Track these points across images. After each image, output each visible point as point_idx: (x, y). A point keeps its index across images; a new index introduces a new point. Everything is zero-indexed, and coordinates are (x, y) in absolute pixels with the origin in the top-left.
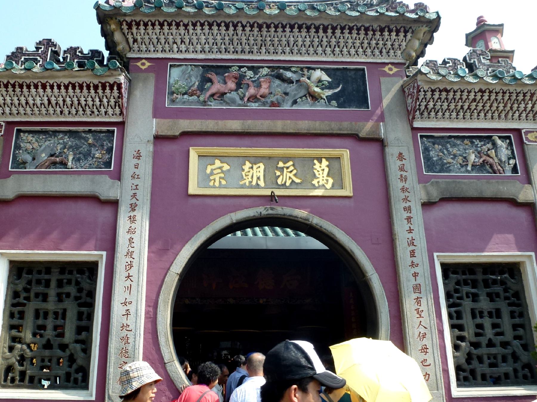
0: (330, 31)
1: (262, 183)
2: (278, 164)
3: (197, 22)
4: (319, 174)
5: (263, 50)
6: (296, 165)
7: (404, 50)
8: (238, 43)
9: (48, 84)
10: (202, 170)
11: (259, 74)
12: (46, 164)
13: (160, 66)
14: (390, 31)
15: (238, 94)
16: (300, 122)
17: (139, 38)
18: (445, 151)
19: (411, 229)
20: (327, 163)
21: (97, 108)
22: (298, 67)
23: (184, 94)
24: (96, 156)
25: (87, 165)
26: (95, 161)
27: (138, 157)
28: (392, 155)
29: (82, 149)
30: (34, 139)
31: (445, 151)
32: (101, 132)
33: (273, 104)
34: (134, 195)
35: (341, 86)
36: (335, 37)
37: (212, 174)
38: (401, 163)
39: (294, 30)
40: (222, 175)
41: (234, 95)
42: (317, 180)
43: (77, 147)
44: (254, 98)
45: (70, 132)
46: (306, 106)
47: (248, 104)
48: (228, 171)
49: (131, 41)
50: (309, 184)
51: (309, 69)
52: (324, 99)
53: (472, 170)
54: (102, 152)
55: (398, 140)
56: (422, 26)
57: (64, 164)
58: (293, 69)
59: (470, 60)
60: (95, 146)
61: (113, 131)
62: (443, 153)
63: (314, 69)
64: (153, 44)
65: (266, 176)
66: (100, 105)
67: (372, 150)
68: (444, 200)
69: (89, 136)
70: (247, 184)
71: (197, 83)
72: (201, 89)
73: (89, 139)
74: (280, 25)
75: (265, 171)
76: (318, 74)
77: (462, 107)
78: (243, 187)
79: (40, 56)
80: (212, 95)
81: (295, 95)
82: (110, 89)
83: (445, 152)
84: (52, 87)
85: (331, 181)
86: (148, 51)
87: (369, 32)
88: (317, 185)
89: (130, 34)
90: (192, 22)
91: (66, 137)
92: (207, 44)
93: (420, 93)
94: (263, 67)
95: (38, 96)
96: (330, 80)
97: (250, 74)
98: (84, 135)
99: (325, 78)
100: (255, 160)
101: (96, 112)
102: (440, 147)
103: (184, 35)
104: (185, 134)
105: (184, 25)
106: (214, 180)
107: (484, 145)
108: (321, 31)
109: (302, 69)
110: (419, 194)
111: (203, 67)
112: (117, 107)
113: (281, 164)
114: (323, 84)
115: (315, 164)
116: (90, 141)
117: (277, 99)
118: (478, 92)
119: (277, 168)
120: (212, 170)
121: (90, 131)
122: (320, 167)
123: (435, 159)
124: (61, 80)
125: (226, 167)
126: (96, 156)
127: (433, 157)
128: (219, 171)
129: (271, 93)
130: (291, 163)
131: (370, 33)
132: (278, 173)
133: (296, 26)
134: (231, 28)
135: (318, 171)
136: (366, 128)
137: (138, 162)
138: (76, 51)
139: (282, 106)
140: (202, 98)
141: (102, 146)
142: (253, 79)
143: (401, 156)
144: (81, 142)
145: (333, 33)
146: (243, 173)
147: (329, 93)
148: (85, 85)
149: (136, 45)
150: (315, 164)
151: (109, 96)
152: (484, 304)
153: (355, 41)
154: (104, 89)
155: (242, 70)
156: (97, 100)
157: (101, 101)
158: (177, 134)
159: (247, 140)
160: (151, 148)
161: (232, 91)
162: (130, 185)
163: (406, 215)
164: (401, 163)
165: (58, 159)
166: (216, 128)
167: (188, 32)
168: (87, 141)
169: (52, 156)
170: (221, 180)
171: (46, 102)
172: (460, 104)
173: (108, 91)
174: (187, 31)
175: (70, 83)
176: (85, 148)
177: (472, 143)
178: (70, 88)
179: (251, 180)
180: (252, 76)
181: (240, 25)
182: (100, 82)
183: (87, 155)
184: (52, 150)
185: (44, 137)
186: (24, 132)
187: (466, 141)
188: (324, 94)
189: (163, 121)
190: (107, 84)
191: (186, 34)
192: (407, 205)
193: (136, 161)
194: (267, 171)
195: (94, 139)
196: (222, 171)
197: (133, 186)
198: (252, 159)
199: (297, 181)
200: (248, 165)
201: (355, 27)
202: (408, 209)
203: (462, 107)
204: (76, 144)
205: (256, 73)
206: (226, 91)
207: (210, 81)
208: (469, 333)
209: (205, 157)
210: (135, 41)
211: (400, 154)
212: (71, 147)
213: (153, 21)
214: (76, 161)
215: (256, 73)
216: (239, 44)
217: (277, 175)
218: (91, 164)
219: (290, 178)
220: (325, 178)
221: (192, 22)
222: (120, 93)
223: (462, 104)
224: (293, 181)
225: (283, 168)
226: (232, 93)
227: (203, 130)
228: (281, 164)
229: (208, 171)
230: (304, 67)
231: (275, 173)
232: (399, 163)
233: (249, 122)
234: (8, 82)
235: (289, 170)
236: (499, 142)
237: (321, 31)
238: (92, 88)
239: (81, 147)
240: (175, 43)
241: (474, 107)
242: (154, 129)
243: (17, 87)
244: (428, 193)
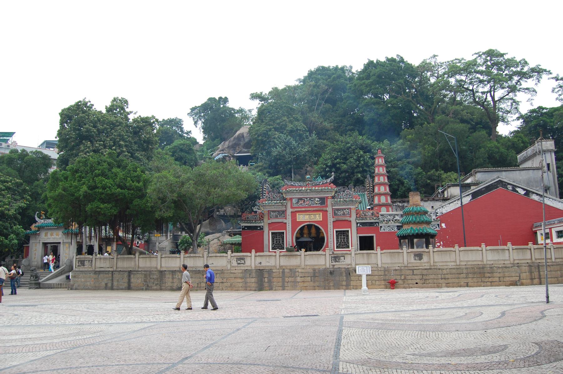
13: (291, 199)
19: (330, 226)
76: (317, 199)
110: (332, 220)
136: (324, 209)
152: (342, 237)
208: (339, 241)
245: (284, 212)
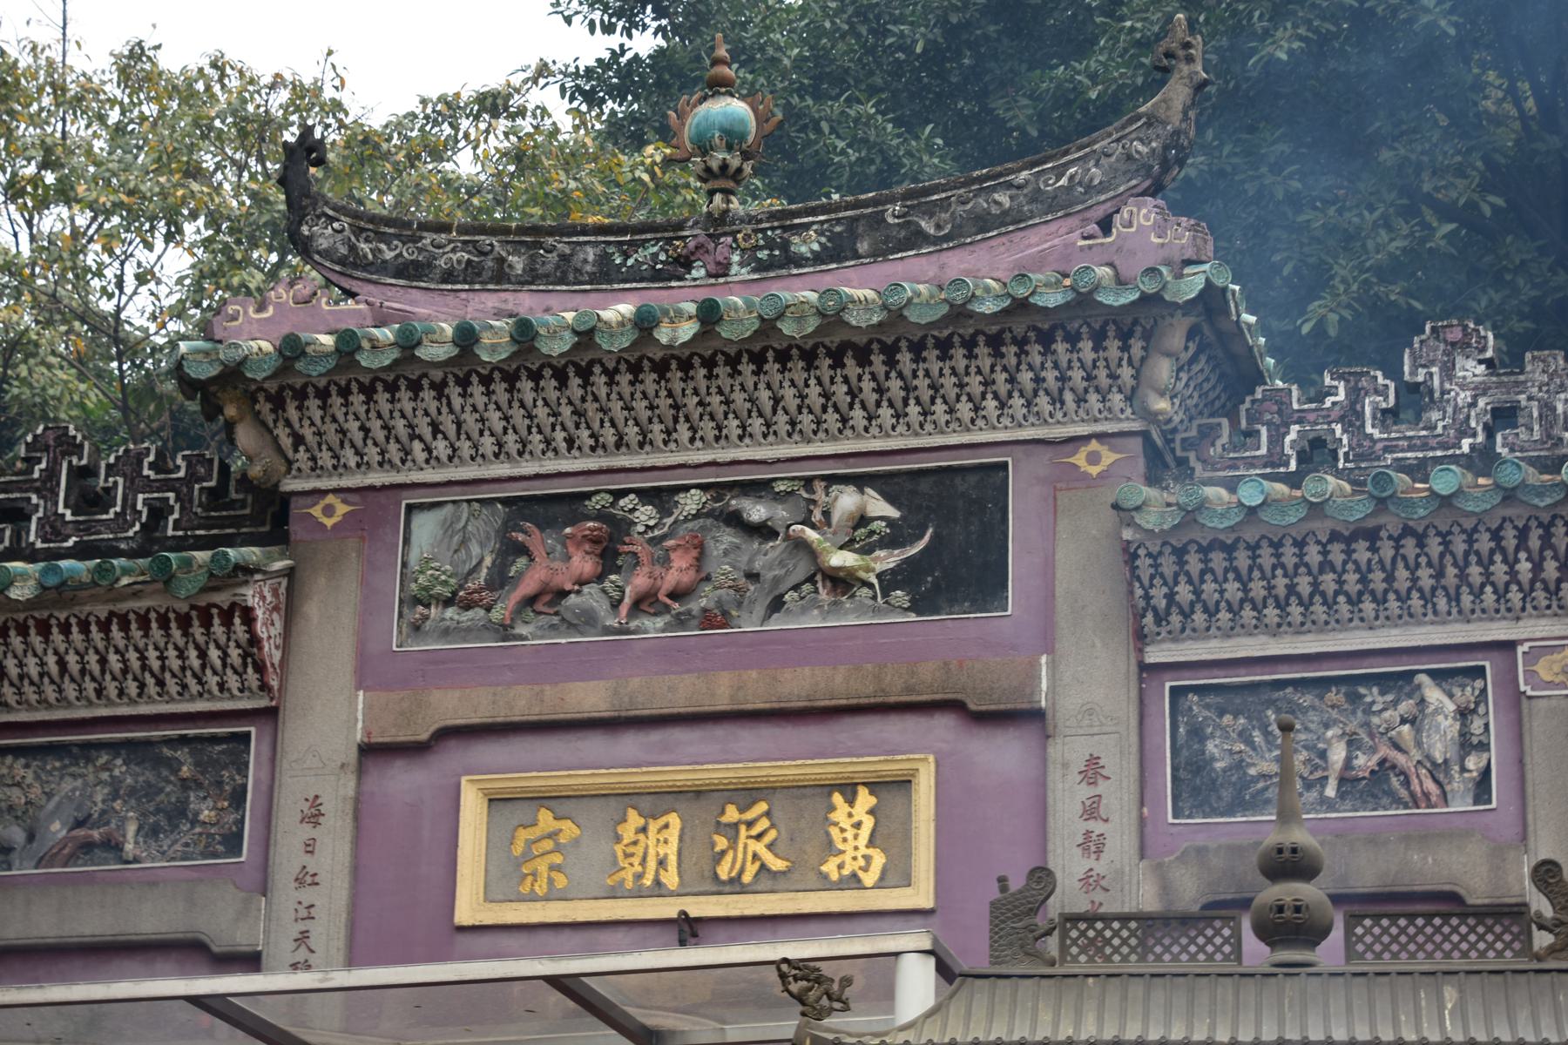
1: (671, 879)
2: (723, 812)
3: (469, 374)
4: (845, 840)
5: (683, 432)
6: (776, 814)
7: (1134, 389)
8: (602, 421)
9: (53, 621)
10: (496, 844)
11: (676, 512)
12: (66, 851)
15: (604, 591)
16: (787, 674)
17: (308, 432)
18: (1256, 733)
20: (873, 801)
21: (195, 675)
22: (793, 479)
23: (448, 602)
24: (202, 817)
25: (178, 847)
26: (200, 834)
27: (314, 817)
28: (1065, 765)
29: (162, 797)
31: (1256, 733)
32: (214, 739)
33: (708, 620)
34: (303, 937)
35: (930, 531)
36: (900, 375)
37: (527, 857)
38: (1092, 791)
39: (766, 367)
40: (557, 859)
41: (592, 598)
42: (837, 860)
43: (150, 791)
44: (645, 603)
47: (633, 624)
48: (576, 842)
49: (286, 442)
50: (812, 876)
51: (832, 480)
52: (871, 586)
53: (1342, 795)
54: (219, 805)
55: (1090, 712)
56: (1172, 316)
57: (112, 846)
58: (781, 487)
59: (1413, 373)
60: (199, 786)
61: (248, 734)
62: (1249, 742)
64: (353, 446)
65: (685, 853)
66: (203, 666)
69: (182, 754)
70: (629, 884)
71: (488, 561)
72: (500, 580)
73: (181, 764)
74: (720, 358)
75: (681, 839)
77: (1291, 589)
78: (614, 894)
79: (37, 491)
80: (530, 601)
81: (777, 581)
82: (222, 624)
83: (1258, 737)
84: (65, 629)
85: (879, 860)
86: (339, 467)
87: (1004, 349)
88: (834, 876)
89: (281, 424)
90: (455, 376)
91: (119, 762)
92: (510, 431)
93: (1138, 563)
94: (686, 488)
95: (29, 654)
96: (893, 513)
97: (645, 514)
98: (167, 752)
99: (879, 507)
100: (656, 801)
101: (194, 687)
102: (1242, 721)
103: (440, 413)
104: (449, 733)
105: (433, 386)
106: (534, 874)
107: (1395, 703)
108: (849, 362)
109: (808, 482)
111: (506, 502)
112: (250, 670)
113: (732, 814)
114: (872, 533)
115: (832, 808)
116: (185, 771)
117: (719, 603)
118: (1330, 541)
119: (720, 828)
121: (184, 740)
122: (850, 815)
123: (1219, 765)
124: (87, 608)
125: (569, 829)
126: (202, 817)
127: (1213, 759)
128: (548, 845)
129: (708, 578)
130: (762, 807)
132: (721, 843)
133: (770, 355)
134: (575, 382)
135: (843, 830)
137: (314, 833)
138: (140, 463)
139: (735, 622)
140: (496, 615)
141: (219, 784)
142: (657, 533)
143: (1093, 770)
144: (159, 775)
145: (891, 363)
146: (619, 849)
147: (887, 560)
148: (153, 615)
149: (302, 454)
150: (832, 808)
151: (222, 639)
153: (966, 380)
154: (207, 624)
155: (622, 503)
156: (193, 654)
157: (203, 655)
159: (630, 743)
160: (349, 785)
161: (587, 582)
162: (292, 905)
164: (1092, 791)
165: (96, 834)
166: (537, 710)
167: (449, 404)
168: (176, 771)
169: (79, 824)
170: (553, 874)
171: (53, 668)
172: (1281, 582)
173: (218, 629)
174: (444, 401)
175: (112, 614)
177: (1355, 698)
178: (114, 628)
179: (640, 869)
180: (652, 523)
181: (597, 369)
182: (193, 607)
183: (179, 813)
184: (78, 809)
185: (57, 764)
187: (1333, 696)
188: (868, 570)
190: (215, 611)
191: (445, 410)
193: (307, 831)
194: (687, 838)
195: (197, 764)
196: (557, 844)
197: (300, 908)
198: (646, 803)
199: (777, 864)
200: (635, 820)
201: (956, 339)
203: (1291, 589)
204: (147, 782)
205: (665, 511)
206: (568, 587)
207: (523, 550)
209: (509, 804)
210: (298, 440)
211: (1093, 761)
212: (132, 792)
213: (343, 383)
214: (146, 836)
215: (665, 511)
216: (607, 424)
217: (718, 849)
218: (187, 845)
219: (755, 856)
220: (863, 850)
221: (455, 376)
222: (251, 631)
223: (1286, 581)
224: (763, 867)
225: (735, 826)
226: (586, 589)
227: (499, 720)
228: (732, 814)
229: (518, 849)
230: (815, 477)
231: (713, 844)
232: (1085, 792)
235: (754, 832)
236: (1433, 694)
237: (849, 362)
238: (173, 625)
239: (161, 790)
240: (413, 437)
241: (1333, 587)
242: (360, 725)
244: (1165, 888)
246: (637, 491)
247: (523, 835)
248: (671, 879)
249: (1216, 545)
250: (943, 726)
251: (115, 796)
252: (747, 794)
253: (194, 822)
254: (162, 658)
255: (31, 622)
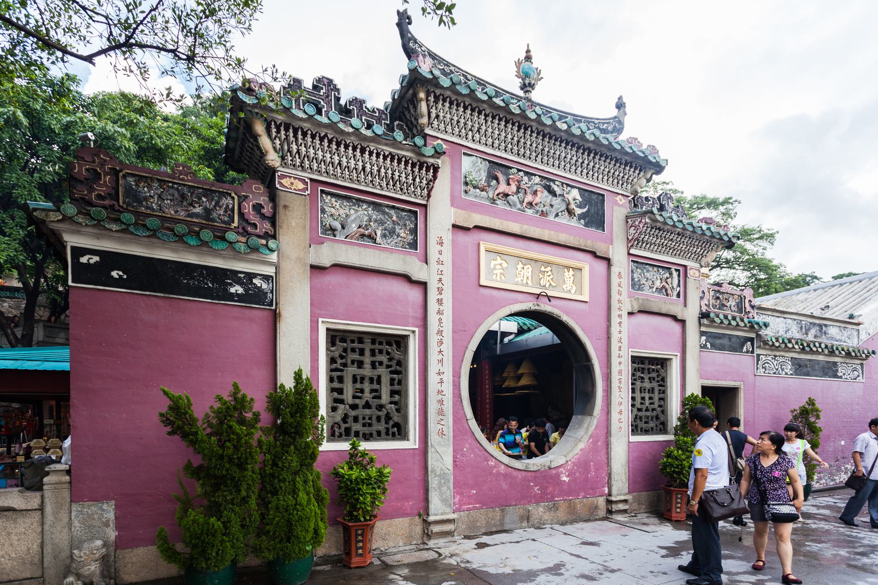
0: (592, 155)
1: (529, 282)
5: (539, 159)
10: (488, 264)
14: (631, 167)
16: (560, 234)
27: (441, 244)
30: (338, 204)
32: (403, 210)
37: (495, 269)
45: (374, 203)
46: (564, 219)
57: (372, 238)
60: (399, 224)
63: (573, 187)
67: (601, 266)
68: (640, 311)
69: (392, 212)
76: (575, 193)
84: (371, 154)
94: (535, 175)
97: (526, 179)
99: (578, 197)
104: (477, 227)
108: (586, 153)
109: (563, 183)
113: (543, 269)
116: (394, 218)
120: (495, 265)
121: (393, 207)
125: (505, 265)
131: (618, 165)
136: (600, 248)
140: (491, 196)
145: (594, 158)
152: (647, 385)
158: (471, 227)
159: (522, 243)
163: (619, 320)
176: (389, 224)
183: (392, 232)
186: (328, 193)
189: (459, 211)
192: (620, 313)
193: (439, 247)
199: (553, 284)
202: (620, 316)
212: (376, 221)
228: (543, 269)
229: (492, 266)
233: (526, 227)
234: (326, 135)
237: (586, 153)
243: (334, 143)
245: (415, 213)
246: (524, 172)
247: (493, 263)
248: (529, 282)
249: (660, 229)
250: (588, 257)
251: (370, 221)
252: (548, 263)
253: (398, 236)
254: (399, 176)
255: (359, 146)
